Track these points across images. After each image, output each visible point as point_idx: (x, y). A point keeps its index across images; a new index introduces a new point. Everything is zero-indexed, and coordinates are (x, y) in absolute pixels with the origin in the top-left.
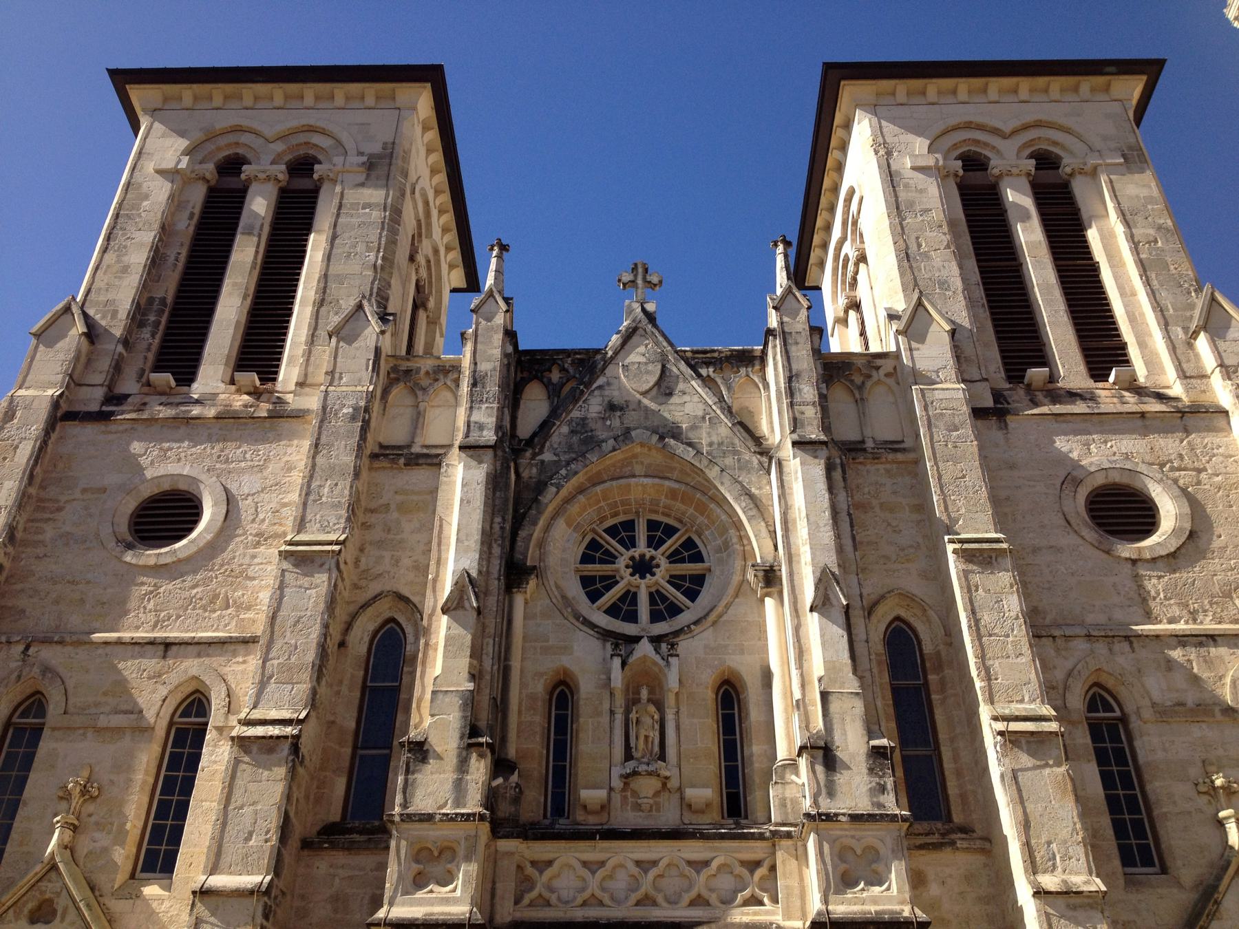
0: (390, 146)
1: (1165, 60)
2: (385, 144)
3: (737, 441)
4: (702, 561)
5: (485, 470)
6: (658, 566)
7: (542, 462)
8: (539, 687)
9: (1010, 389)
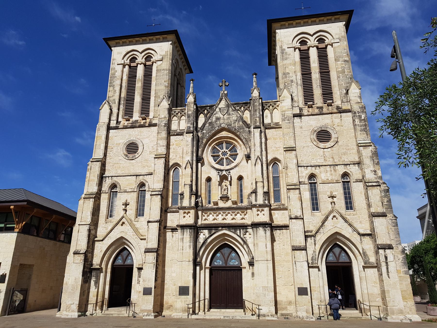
0: (167, 52)
2: (166, 51)
3: (243, 125)
4: (237, 152)
5: (192, 137)
6: (228, 153)
7: (203, 133)
8: (204, 180)
9: (304, 107)
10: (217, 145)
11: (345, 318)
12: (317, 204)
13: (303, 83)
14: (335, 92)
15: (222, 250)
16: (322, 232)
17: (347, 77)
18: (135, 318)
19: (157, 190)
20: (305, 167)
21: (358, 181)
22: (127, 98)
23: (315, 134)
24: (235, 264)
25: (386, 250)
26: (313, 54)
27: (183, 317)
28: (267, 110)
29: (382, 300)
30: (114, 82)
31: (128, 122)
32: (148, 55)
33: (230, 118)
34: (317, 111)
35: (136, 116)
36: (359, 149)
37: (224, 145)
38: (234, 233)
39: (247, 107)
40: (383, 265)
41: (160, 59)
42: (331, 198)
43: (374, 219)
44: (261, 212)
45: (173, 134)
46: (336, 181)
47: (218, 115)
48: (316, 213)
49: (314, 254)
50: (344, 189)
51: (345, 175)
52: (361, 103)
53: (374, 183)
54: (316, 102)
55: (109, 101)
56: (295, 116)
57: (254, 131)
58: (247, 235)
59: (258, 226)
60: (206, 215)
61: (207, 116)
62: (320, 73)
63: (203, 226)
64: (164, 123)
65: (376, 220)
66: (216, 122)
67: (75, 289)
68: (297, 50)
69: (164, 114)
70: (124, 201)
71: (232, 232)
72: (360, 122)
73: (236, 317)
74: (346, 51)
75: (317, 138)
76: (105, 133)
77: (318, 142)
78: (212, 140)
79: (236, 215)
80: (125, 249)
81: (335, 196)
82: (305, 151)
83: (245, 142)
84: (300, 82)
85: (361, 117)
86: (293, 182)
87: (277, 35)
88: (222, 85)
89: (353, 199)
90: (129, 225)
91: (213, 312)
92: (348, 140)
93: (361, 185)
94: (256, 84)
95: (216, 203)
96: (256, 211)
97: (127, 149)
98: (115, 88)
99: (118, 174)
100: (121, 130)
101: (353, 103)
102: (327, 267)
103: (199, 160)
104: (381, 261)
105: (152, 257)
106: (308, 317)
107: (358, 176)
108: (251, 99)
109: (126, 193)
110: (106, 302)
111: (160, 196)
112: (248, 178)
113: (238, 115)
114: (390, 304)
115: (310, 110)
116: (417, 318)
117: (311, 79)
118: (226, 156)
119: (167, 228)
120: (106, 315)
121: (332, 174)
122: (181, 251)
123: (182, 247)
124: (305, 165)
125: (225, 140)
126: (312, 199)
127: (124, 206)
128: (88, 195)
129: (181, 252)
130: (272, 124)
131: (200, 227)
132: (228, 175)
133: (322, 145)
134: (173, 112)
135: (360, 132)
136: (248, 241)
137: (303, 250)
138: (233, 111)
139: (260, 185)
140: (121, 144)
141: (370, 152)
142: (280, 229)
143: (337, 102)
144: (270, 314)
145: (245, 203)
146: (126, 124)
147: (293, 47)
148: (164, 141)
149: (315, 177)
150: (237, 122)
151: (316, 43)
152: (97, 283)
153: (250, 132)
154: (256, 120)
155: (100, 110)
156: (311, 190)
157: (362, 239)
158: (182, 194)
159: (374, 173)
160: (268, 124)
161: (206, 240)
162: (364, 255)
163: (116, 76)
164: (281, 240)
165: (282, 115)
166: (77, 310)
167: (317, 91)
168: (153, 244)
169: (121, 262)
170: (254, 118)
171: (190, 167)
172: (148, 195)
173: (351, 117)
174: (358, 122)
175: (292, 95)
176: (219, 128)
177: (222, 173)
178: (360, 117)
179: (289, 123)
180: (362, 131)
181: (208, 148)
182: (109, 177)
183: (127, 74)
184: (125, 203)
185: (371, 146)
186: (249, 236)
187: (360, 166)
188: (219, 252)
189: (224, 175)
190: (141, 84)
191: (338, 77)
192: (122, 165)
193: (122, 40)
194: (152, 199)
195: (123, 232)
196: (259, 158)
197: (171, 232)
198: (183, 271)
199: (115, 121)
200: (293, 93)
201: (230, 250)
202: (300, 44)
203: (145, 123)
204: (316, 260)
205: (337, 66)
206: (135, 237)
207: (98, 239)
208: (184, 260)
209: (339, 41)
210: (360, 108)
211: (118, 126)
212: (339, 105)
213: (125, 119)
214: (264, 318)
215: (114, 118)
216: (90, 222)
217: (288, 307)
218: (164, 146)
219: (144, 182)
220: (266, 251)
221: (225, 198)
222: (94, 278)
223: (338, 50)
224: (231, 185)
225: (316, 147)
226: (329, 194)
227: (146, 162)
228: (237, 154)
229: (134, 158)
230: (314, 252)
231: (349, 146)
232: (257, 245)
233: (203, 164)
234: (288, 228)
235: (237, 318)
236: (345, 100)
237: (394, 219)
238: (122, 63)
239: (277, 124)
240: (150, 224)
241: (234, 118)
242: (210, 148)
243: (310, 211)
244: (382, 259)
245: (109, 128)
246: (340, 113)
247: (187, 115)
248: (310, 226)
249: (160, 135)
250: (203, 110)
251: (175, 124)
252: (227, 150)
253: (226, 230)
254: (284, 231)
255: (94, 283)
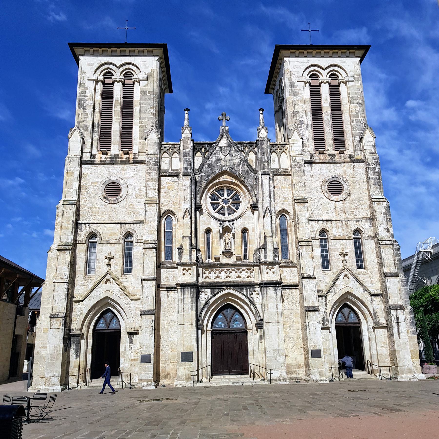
1: (370, 46)
2: (151, 69)
3: (248, 170)
4: (240, 200)
5: (190, 180)
6: (229, 201)
7: (202, 175)
9: (315, 153)
10: (218, 190)
11: (356, 380)
12: (327, 262)
13: (313, 125)
14: (348, 138)
15: (224, 312)
16: (333, 291)
17: (361, 122)
18: (132, 389)
19: (150, 242)
20: (316, 222)
21: (370, 238)
22: (102, 124)
23: (326, 185)
24: (239, 326)
25: (398, 311)
26: (325, 90)
27: (188, 386)
28: (274, 153)
29: (391, 361)
30: (84, 102)
31: (105, 155)
32: (127, 71)
33: (233, 160)
34: (328, 159)
35: (115, 149)
36: (372, 204)
37: (225, 191)
38: (241, 293)
39: (252, 147)
40: (395, 325)
41: (144, 79)
42: (342, 256)
43: (386, 279)
44: (270, 270)
45: (163, 175)
46: (348, 237)
47: (219, 156)
48: (327, 271)
49: (325, 315)
50: (355, 246)
51: (357, 231)
52: (376, 153)
53: (387, 242)
54: (327, 148)
55: (79, 127)
56: (306, 162)
57: (262, 178)
58: (254, 296)
59: (268, 286)
60: (207, 272)
61: (205, 155)
62: (332, 115)
63: (204, 284)
64: (154, 160)
65: (388, 280)
66: (216, 163)
67: (55, 359)
68: (308, 85)
69: (153, 149)
70: (107, 254)
71: (238, 291)
72: (374, 175)
73: (246, 382)
74: (360, 92)
75: (329, 189)
76: (77, 168)
77: (329, 194)
78: (211, 185)
79: (241, 272)
80: (108, 310)
81: (347, 254)
82: (316, 204)
83: (251, 190)
84: (310, 123)
85: (375, 169)
86: (305, 238)
87: (285, 64)
88: (222, 119)
89: (365, 257)
90: (115, 283)
91: (217, 379)
92: (361, 194)
93: (373, 242)
94: (263, 122)
95: (217, 259)
96: (265, 269)
97: (106, 189)
98: (86, 111)
99: (97, 221)
100: (97, 165)
101: (367, 152)
102: (337, 328)
103: (198, 208)
104: (393, 322)
105: (149, 320)
106: (321, 379)
107: (370, 233)
108: (258, 140)
109: (108, 244)
110: (88, 373)
111: (154, 249)
112: (254, 231)
113: (242, 156)
114: (400, 364)
115: (322, 156)
116: (422, 377)
117: (322, 121)
118: (227, 205)
119: (161, 286)
120: (93, 388)
121: (343, 230)
122: (182, 313)
123: (182, 309)
124: (316, 219)
125: (227, 185)
126: (323, 256)
127: (107, 260)
128: (62, 247)
129: (181, 314)
130: (280, 170)
131: (201, 286)
132: (231, 227)
133: (333, 197)
134: (163, 148)
135: (374, 186)
136: (255, 301)
137: (316, 311)
138: (237, 151)
139: (269, 240)
140: (99, 184)
141: (384, 208)
142: (289, 288)
143: (350, 150)
144: (281, 378)
145: (250, 259)
146: (103, 159)
147: (304, 81)
148: (155, 183)
149: (326, 233)
150: (241, 166)
151: (329, 79)
152: (78, 351)
153: (256, 178)
154: (264, 165)
155: (69, 138)
156: (322, 246)
157: (373, 299)
158: (180, 248)
159: (386, 230)
160: (276, 170)
161: (208, 300)
162: (374, 316)
163: (86, 94)
164: (290, 300)
165: (293, 161)
166: (59, 383)
167: (329, 136)
168: (150, 305)
169: (103, 326)
170: (261, 162)
171: (188, 216)
172: (137, 249)
173: (364, 168)
174: (372, 175)
175: (302, 138)
176: (221, 171)
177: (225, 224)
178: (374, 169)
179: (300, 170)
180: (376, 185)
181: (207, 194)
182: (85, 224)
183: (100, 93)
184: (109, 257)
185: (385, 202)
186: (257, 297)
187: (372, 222)
188: (221, 314)
189: (227, 226)
190: (119, 108)
191: (352, 122)
192: (100, 210)
193: (94, 48)
194: (146, 253)
195: (109, 291)
196: (269, 209)
197: (166, 292)
198: (185, 335)
199: (88, 153)
200: (303, 135)
201: (234, 311)
202: (311, 78)
203: (128, 159)
204: (327, 321)
205: (351, 109)
206: (123, 297)
207: (77, 300)
208: (186, 322)
209: (353, 80)
210: (374, 159)
211: (94, 161)
212: (352, 154)
213: (102, 151)
214: (275, 383)
215: (87, 149)
216: (68, 279)
217: (298, 370)
218: (154, 189)
219: (131, 231)
220: (277, 312)
221: (228, 253)
222: (74, 345)
223: (352, 90)
224: (234, 238)
225: (328, 199)
226: (340, 251)
227: (132, 208)
228: (241, 202)
229: (117, 202)
230: (325, 312)
231: (361, 200)
232: (267, 306)
233: (201, 213)
234: (297, 287)
235: (247, 384)
236: (358, 148)
237: (404, 279)
238: (94, 78)
239: (285, 170)
240: (144, 282)
241: (238, 160)
242: (209, 194)
243: (321, 269)
244: (394, 320)
245: (82, 163)
246: (353, 163)
247: (183, 154)
248: (321, 285)
249: (150, 175)
250: (200, 147)
251: (166, 162)
252: (228, 197)
253: (231, 289)
254: (293, 290)
255: (75, 351)
